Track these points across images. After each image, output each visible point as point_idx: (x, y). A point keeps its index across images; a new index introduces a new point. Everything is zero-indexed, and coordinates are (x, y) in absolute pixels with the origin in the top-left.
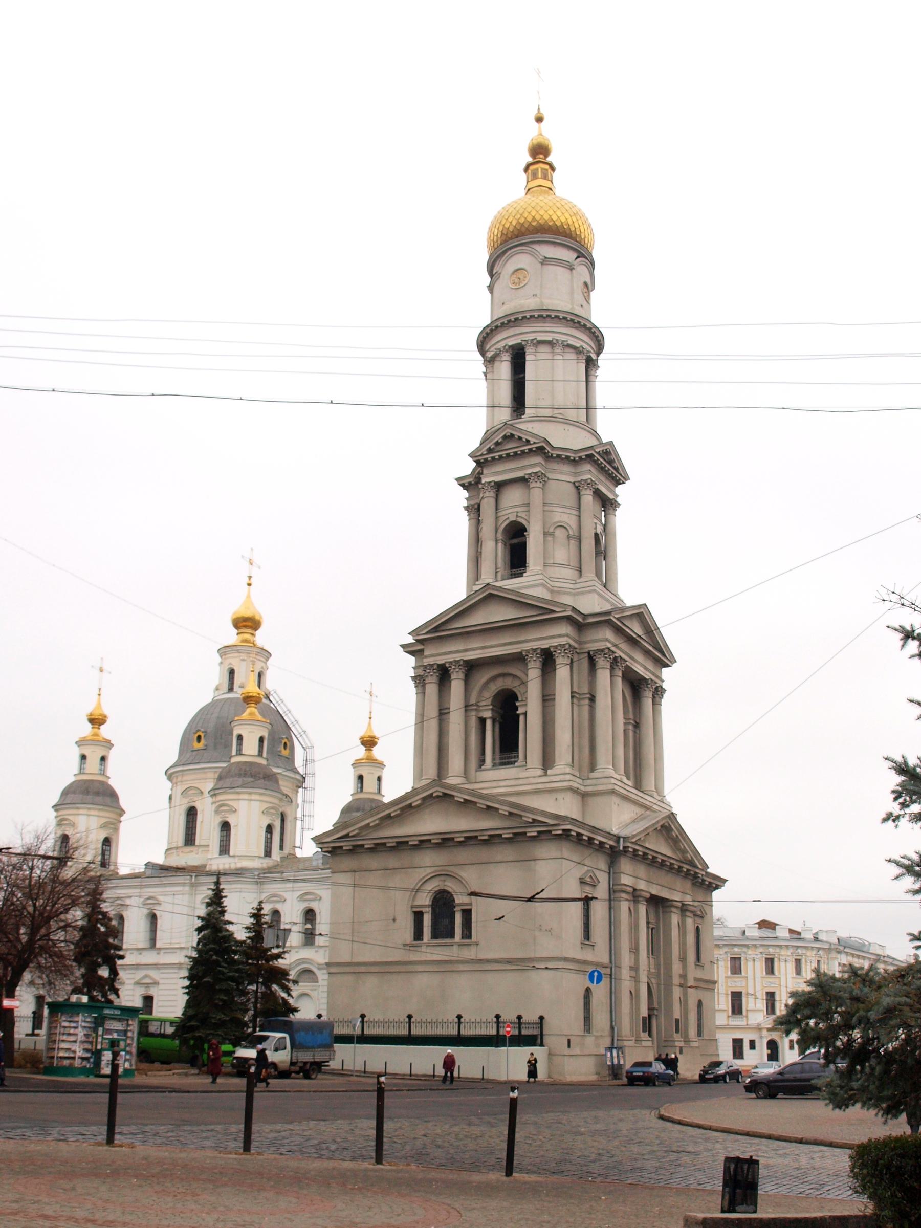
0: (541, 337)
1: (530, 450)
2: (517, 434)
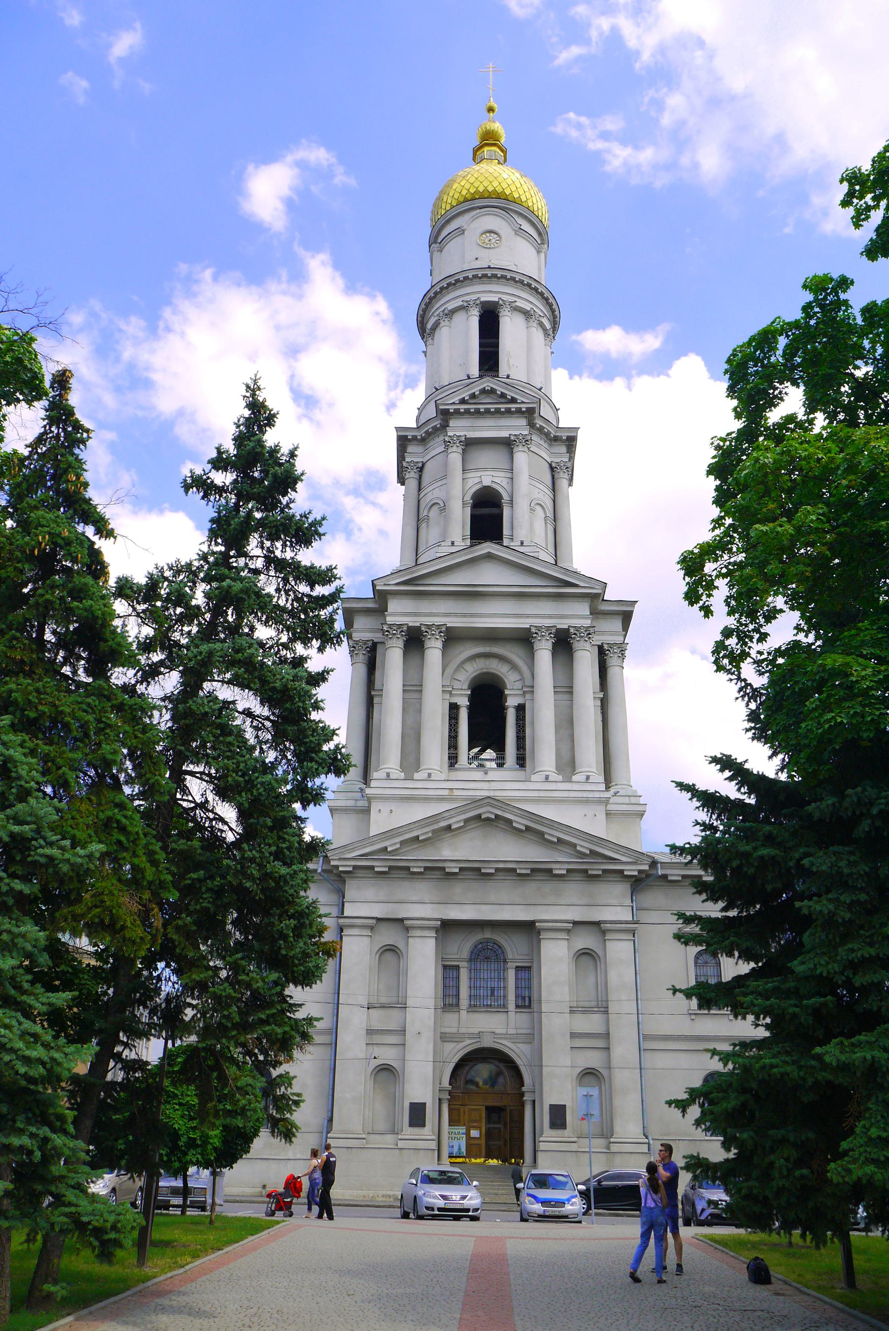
1: (519, 411)
2: (500, 390)
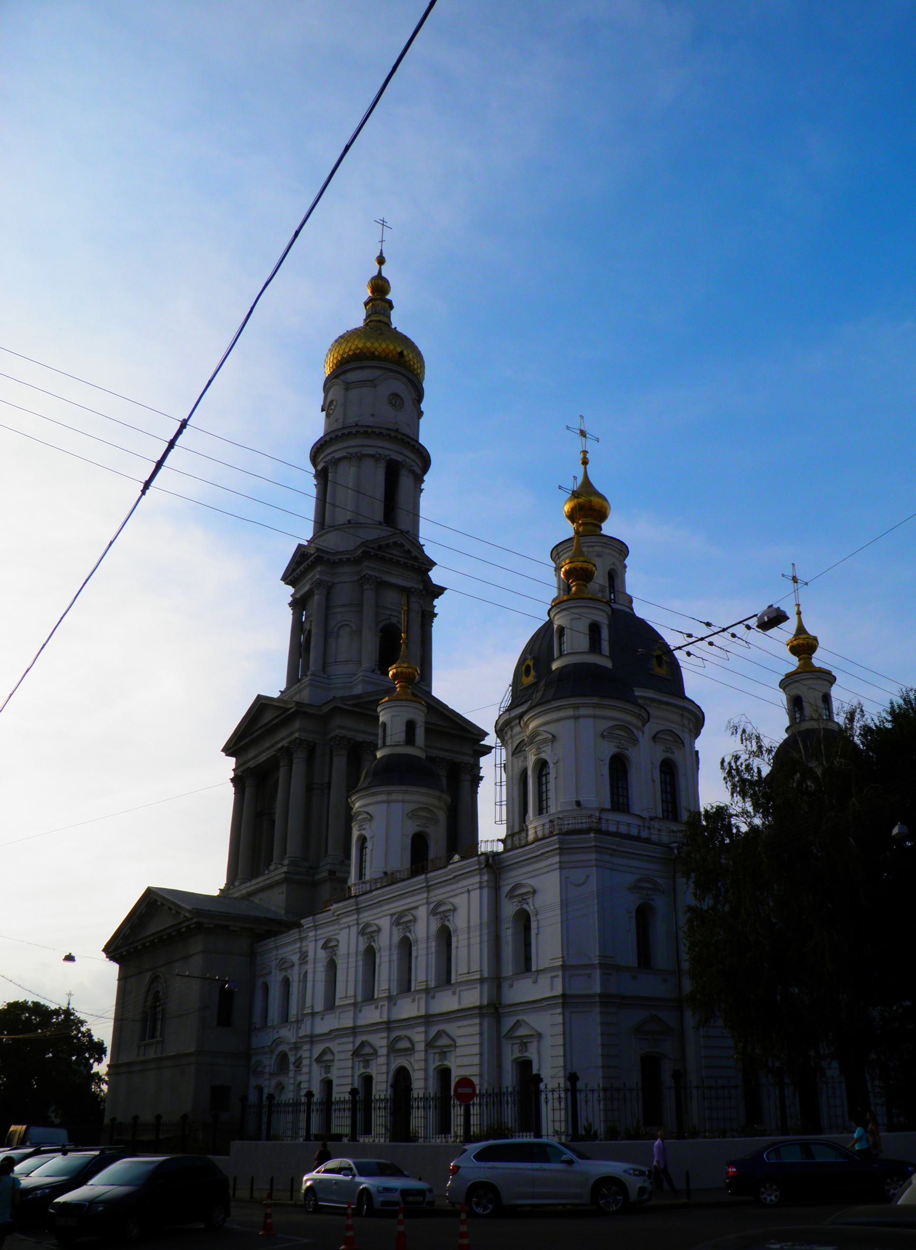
0: (338, 455)
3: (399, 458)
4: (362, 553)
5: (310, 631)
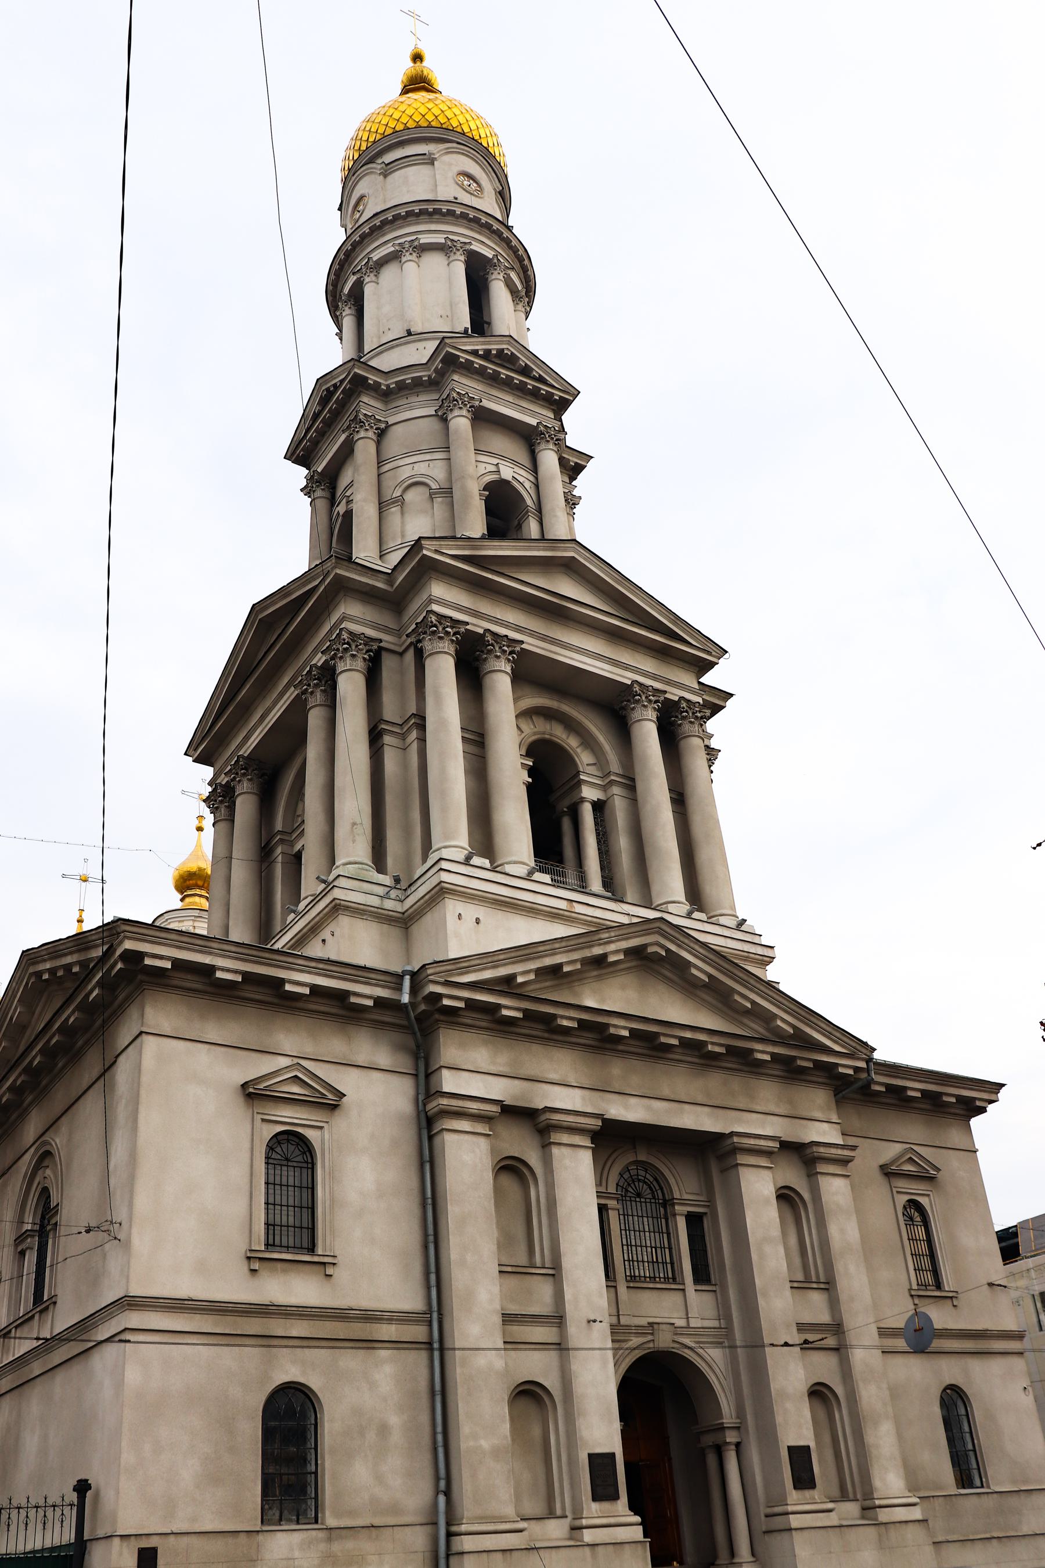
3: (489, 254)
4: (442, 361)
5: (348, 515)
